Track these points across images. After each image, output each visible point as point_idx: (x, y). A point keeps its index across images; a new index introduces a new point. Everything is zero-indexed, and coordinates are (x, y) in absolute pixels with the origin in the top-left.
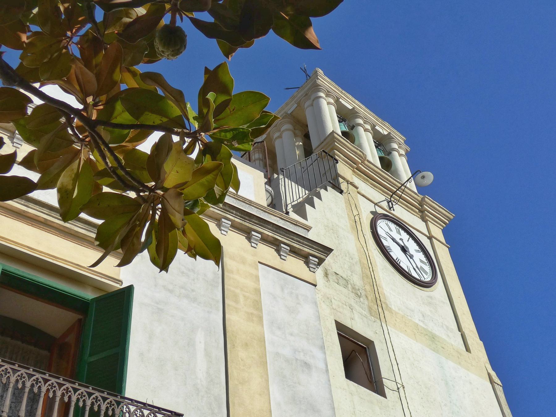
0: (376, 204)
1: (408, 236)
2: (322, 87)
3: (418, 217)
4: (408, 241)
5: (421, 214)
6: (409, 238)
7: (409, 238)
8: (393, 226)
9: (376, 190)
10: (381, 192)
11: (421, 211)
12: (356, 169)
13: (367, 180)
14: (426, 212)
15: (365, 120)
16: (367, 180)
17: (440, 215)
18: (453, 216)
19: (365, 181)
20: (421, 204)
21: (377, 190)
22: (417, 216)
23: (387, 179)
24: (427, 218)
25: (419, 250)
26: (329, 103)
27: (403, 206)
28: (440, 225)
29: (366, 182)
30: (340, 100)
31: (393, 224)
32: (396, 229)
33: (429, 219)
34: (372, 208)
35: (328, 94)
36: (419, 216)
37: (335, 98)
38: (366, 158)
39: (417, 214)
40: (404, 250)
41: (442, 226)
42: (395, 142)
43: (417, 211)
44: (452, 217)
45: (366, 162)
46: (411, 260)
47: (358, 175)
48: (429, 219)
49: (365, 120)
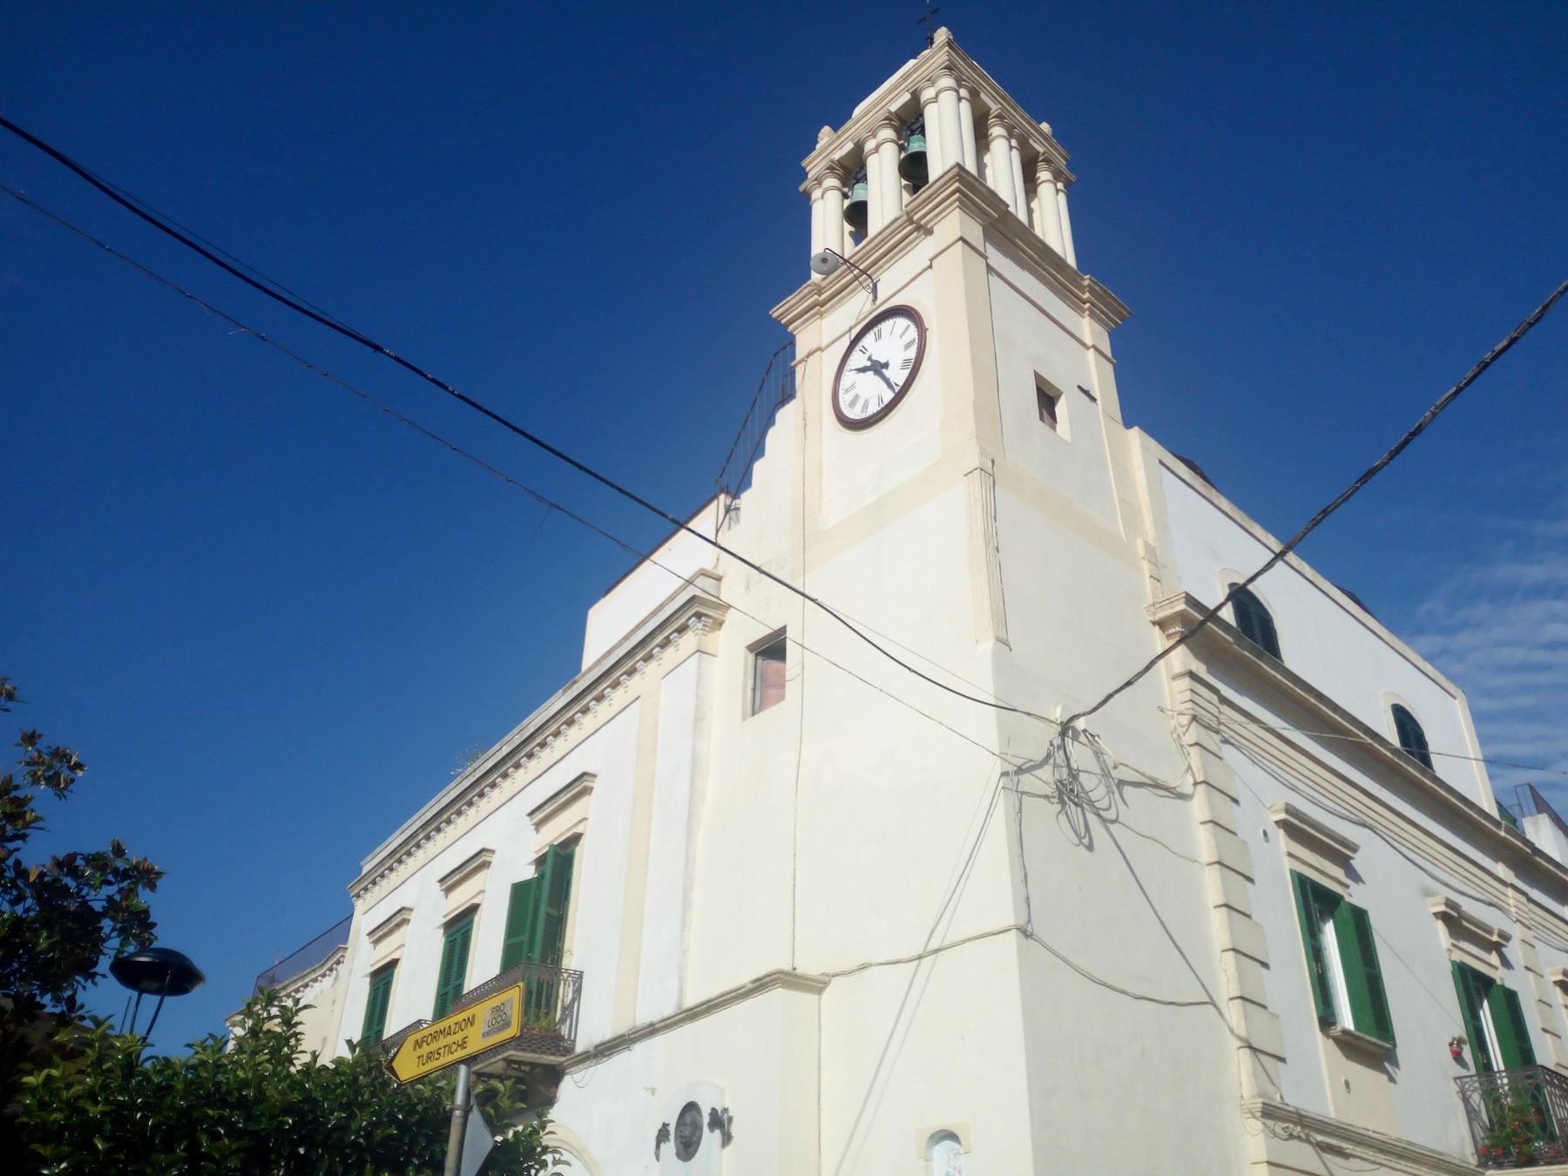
0: (851, 329)
5: (922, 232)
11: (919, 228)
12: (822, 306)
13: (842, 298)
14: (922, 222)
16: (842, 298)
17: (941, 193)
20: (911, 224)
22: (921, 241)
23: (868, 253)
24: (929, 226)
27: (896, 258)
28: (951, 204)
30: (837, 156)
34: (844, 343)
36: (923, 236)
38: (816, 284)
40: (877, 368)
41: (955, 201)
42: (921, 90)
43: (915, 234)
45: (824, 284)
47: (833, 306)
48: (933, 223)
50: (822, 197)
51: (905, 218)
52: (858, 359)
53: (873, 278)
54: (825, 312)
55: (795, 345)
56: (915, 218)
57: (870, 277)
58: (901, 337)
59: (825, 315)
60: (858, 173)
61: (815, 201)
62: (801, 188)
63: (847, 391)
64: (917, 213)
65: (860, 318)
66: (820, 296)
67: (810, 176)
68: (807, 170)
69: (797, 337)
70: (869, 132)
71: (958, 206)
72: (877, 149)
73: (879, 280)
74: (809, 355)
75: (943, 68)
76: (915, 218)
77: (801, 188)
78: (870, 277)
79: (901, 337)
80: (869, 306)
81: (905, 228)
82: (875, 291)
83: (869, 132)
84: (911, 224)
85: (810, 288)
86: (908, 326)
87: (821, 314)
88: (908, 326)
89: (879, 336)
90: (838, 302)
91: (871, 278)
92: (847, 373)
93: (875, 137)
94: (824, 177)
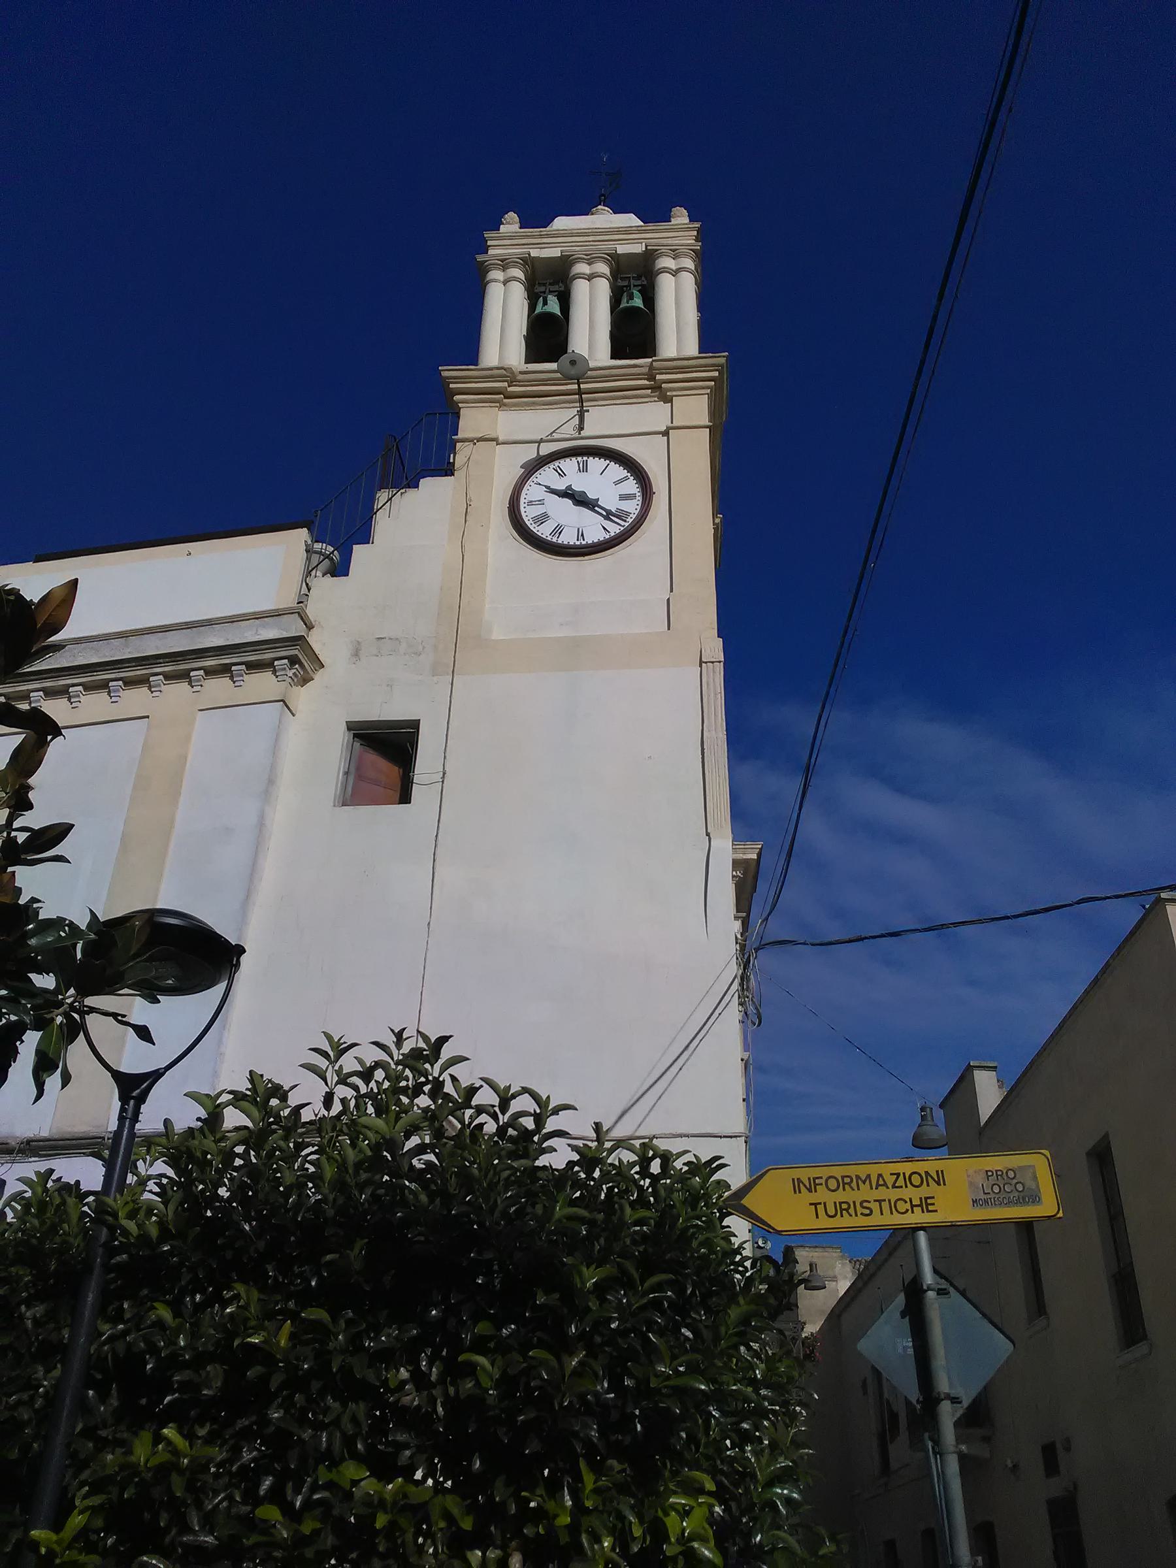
1: (608, 462)
2: (490, 262)
3: (655, 401)
4: (601, 474)
6: (608, 465)
7: (608, 465)
8: (569, 465)
9: (556, 408)
10: (567, 405)
12: (506, 397)
15: (589, 257)
16: (534, 404)
17: (696, 371)
18: (724, 357)
19: (530, 406)
20: (651, 377)
21: (559, 406)
22: (651, 402)
25: (629, 474)
26: (505, 283)
28: (703, 388)
29: (532, 408)
30: (534, 253)
31: (573, 459)
32: (579, 464)
33: (674, 393)
34: (530, 453)
35: (505, 264)
36: (656, 399)
37: (517, 262)
39: (650, 397)
41: (707, 388)
44: (723, 360)
45: (520, 377)
46: (596, 508)
48: (674, 393)
49: (589, 257)
50: (505, 283)
51: (645, 370)
52: (547, 475)
53: (584, 404)
54: (505, 405)
55: (459, 418)
56: (658, 377)
57: (581, 401)
58: (617, 483)
59: (505, 408)
60: (550, 284)
61: (496, 281)
62: (480, 258)
63: (530, 503)
64: (662, 374)
65: (556, 436)
66: (509, 386)
67: (491, 252)
68: (489, 243)
69: (462, 412)
70: (586, 255)
71: (708, 394)
72: (590, 278)
73: (588, 411)
74: (480, 440)
75: (691, 250)
76: (658, 377)
77: (480, 258)
78: (581, 401)
79: (617, 483)
80: (569, 430)
81: (641, 379)
82: (581, 415)
83: (586, 255)
84: (647, 379)
85: (505, 372)
86: (626, 478)
87: (502, 406)
88: (626, 478)
89: (584, 469)
90: (527, 404)
91: (582, 404)
92: (532, 484)
93: (589, 264)
94: (514, 264)
